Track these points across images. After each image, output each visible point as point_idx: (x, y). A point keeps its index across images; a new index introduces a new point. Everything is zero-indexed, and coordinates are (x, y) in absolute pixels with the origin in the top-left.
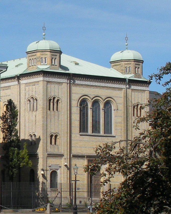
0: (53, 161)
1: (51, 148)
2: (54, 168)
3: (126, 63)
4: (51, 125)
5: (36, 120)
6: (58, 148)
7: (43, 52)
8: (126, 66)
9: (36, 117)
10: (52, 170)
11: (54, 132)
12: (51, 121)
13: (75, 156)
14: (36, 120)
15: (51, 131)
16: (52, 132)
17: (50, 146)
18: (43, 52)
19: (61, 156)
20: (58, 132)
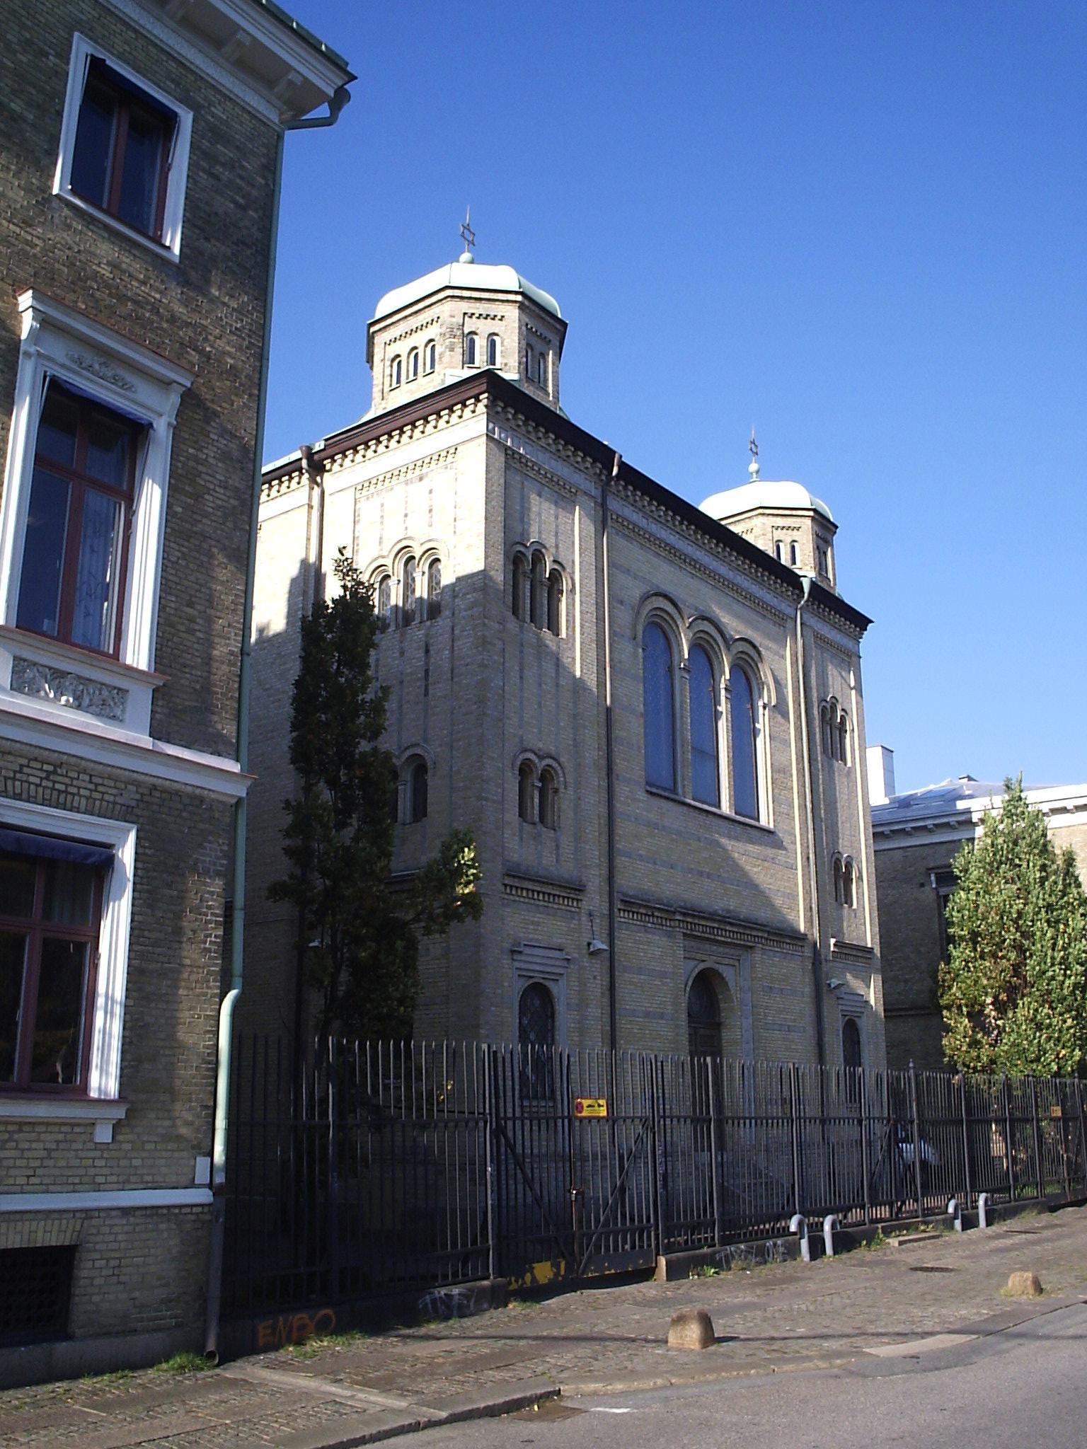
0: (533, 923)
1: (521, 839)
2: (537, 963)
3: (780, 522)
4: (521, 703)
5: (427, 671)
6: (558, 847)
7: (480, 299)
8: (779, 534)
9: (427, 651)
10: (532, 981)
11: (540, 750)
12: (521, 678)
13: (629, 904)
14: (427, 671)
15: (522, 741)
16: (530, 746)
17: (521, 830)
18: (480, 299)
19: (576, 889)
20: (552, 750)
